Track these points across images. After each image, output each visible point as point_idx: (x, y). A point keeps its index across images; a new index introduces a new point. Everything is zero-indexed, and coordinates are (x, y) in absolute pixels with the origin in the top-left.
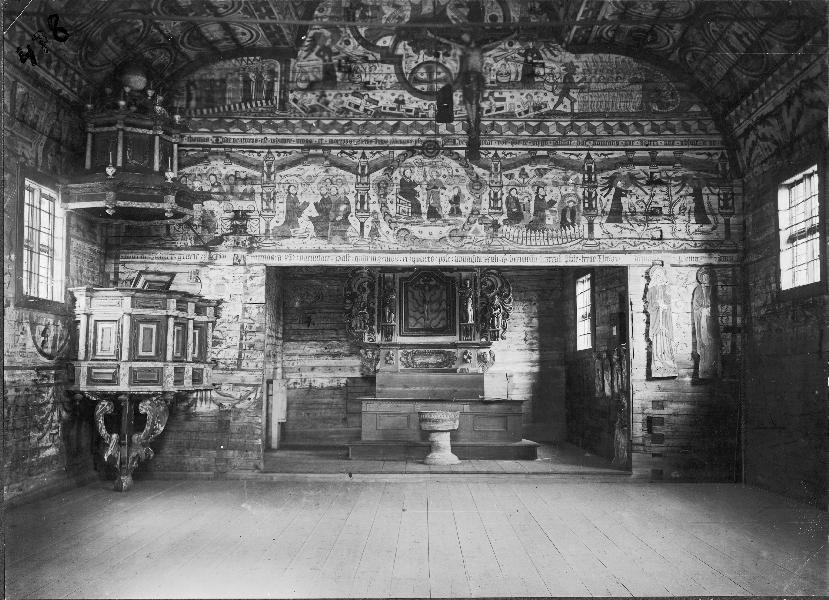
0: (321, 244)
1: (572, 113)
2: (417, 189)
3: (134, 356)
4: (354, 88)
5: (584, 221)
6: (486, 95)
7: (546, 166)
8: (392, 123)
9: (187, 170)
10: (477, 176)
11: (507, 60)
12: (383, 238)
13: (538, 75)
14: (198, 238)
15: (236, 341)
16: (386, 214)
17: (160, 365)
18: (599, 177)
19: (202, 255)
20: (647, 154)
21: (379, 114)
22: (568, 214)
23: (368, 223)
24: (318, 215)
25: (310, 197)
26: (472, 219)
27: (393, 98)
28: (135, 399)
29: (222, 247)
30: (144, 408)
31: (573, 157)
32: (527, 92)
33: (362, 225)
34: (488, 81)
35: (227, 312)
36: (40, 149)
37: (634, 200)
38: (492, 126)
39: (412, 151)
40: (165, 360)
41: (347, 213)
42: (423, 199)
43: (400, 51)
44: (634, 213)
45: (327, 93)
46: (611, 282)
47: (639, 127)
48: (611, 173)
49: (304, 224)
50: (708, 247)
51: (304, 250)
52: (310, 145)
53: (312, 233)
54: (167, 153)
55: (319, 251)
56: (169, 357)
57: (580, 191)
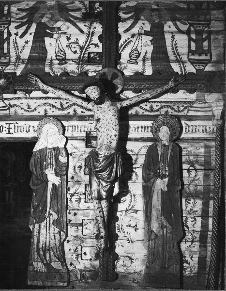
18: (14, 9)
37: (64, 41)
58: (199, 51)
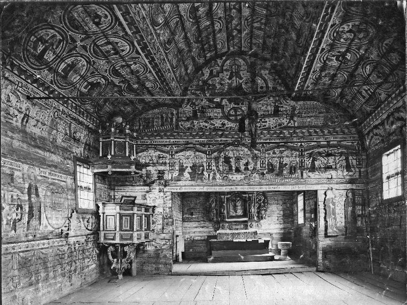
0: (193, 183)
1: (294, 127)
2: (231, 160)
3: (121, 229)
4: (205, 119)
5: (299, 171)
6: (258, 121)
7: (283, 149)
8: (220, 133)
9: (140, 154)
10: (255, 154)
11: (267, 105)
12: (218, 180)
13: (280, 111)
14: (145, 181)
15: (161, 222)
16: (219, 170)
17: (131, 232)
18: (305, 153)
19: (147, 188)
20: (326, 143)
21: (215, 129)
22: (293, 169)
23: (211, 175)
24: (191, 171)
25: (188, 164)
26: (253, 172)
27: (221, 123)
28: (123, 245)
29: (155, 184)
30: (126, 249)
31: (294, 145)
32: (276, 118)
33: (209, 175)
34: (260, 114)
35: (157, 210)
36: (82, 149)
37: (320, 162)
38: (262, 133)
39: (229, 145)
40: (133, 230)
41: (203, 170)
42: (233, 164)
43: (224, 103)
44: (320, 168)
45: (195, 121)
46: (311, 196)
47: (323, 132)
48: (311, 151)
49: (186, 175)
50: (351, 181)
51: (187, 185)
52: (187, 143)
53: (190, 179)
54: (131, 147)
55: (192, 186)
56: (135, 230)
57: (298, 159)
58: (360, 164)
